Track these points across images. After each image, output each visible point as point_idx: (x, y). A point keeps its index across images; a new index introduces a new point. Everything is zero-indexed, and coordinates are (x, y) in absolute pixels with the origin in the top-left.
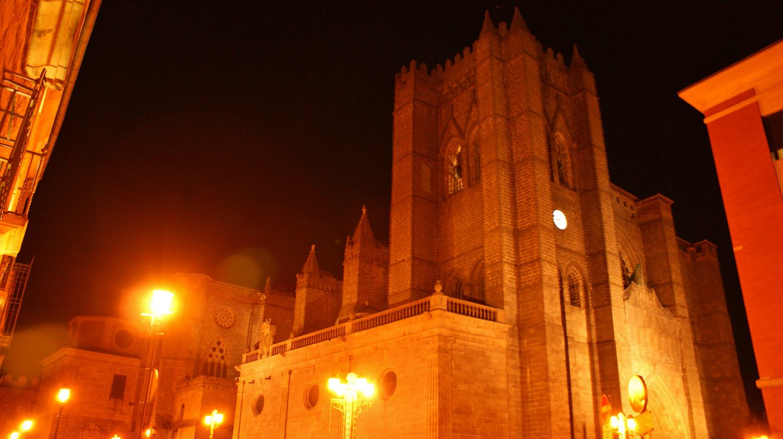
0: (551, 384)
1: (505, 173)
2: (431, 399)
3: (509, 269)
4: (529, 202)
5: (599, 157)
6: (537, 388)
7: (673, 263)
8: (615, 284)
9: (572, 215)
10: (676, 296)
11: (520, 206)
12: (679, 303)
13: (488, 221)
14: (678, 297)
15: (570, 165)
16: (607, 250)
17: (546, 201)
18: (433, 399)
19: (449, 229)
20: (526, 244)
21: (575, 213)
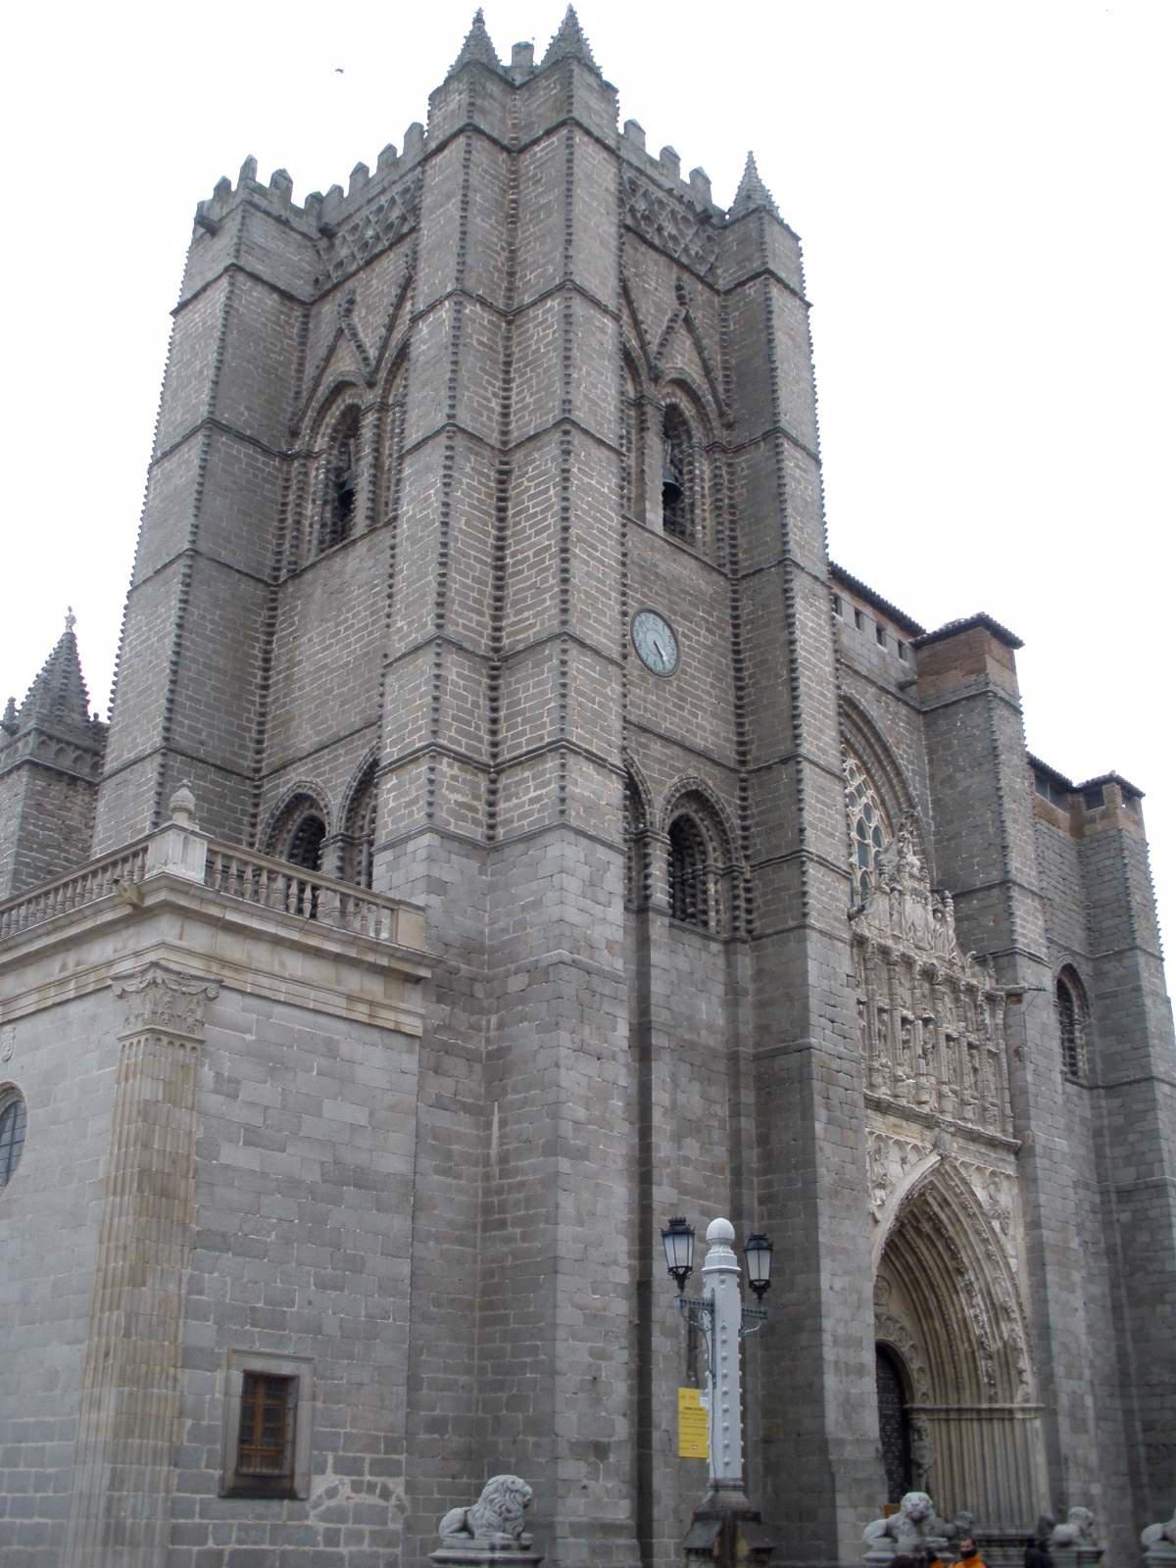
0: (564, 1164)
1: (473, 469)
2: (114, 1194)
3: (456, 771)
4: (543, 561)
5: (797, 466)
6: (519, 1178)
7: (1015, 821)
8: (823, 862)
9: (697, 634)
10: (1018, 921)
12: (1028, 946)
13: (404, 618)
14: (1023, 927)
15: (707, 485)
16: (803, 751)
17: (602, 563)
18: (122, 1195)
19: (300, 662)
20: (522, 695)
21: (708, 630)
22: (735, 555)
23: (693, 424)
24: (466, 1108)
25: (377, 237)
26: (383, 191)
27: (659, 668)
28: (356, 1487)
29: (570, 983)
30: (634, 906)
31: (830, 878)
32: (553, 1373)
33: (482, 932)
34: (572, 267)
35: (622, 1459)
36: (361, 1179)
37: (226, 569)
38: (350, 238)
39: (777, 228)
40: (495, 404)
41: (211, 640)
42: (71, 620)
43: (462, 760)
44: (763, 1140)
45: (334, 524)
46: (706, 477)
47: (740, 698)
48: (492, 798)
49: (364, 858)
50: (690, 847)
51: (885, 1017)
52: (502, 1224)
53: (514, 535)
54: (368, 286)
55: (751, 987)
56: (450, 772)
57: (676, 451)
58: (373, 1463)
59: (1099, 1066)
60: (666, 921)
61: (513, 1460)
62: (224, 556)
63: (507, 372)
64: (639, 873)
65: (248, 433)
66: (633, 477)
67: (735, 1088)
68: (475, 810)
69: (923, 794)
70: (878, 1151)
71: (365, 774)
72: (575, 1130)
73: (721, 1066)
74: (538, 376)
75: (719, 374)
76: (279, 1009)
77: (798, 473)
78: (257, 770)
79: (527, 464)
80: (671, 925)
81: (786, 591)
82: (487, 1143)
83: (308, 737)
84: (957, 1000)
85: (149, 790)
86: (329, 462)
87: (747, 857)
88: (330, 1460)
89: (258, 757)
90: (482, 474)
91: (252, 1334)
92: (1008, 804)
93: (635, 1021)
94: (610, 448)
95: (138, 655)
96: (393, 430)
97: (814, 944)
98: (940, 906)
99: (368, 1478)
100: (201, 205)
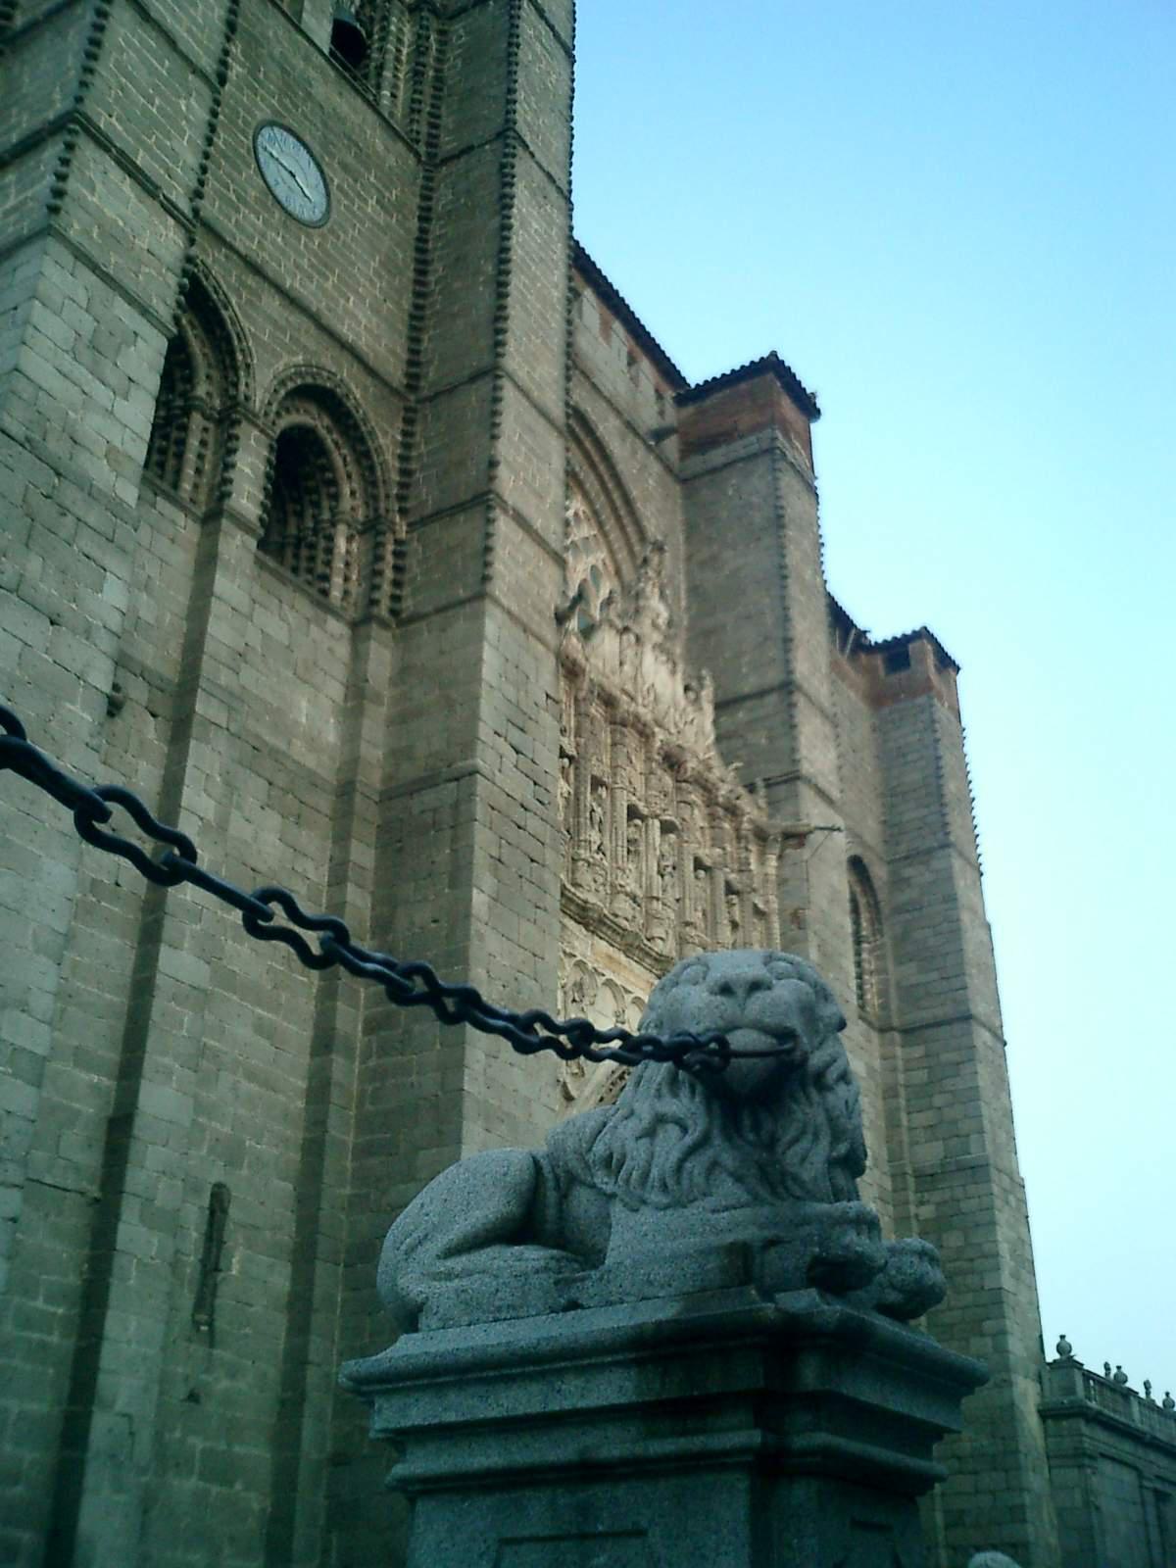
51: (603, 792)
55: (387, 694)
59: (894, 1004)
70: (579, 986)
73: (325, 802)
81: (504, 196)
84: (712, 817)
97: (493, 624)
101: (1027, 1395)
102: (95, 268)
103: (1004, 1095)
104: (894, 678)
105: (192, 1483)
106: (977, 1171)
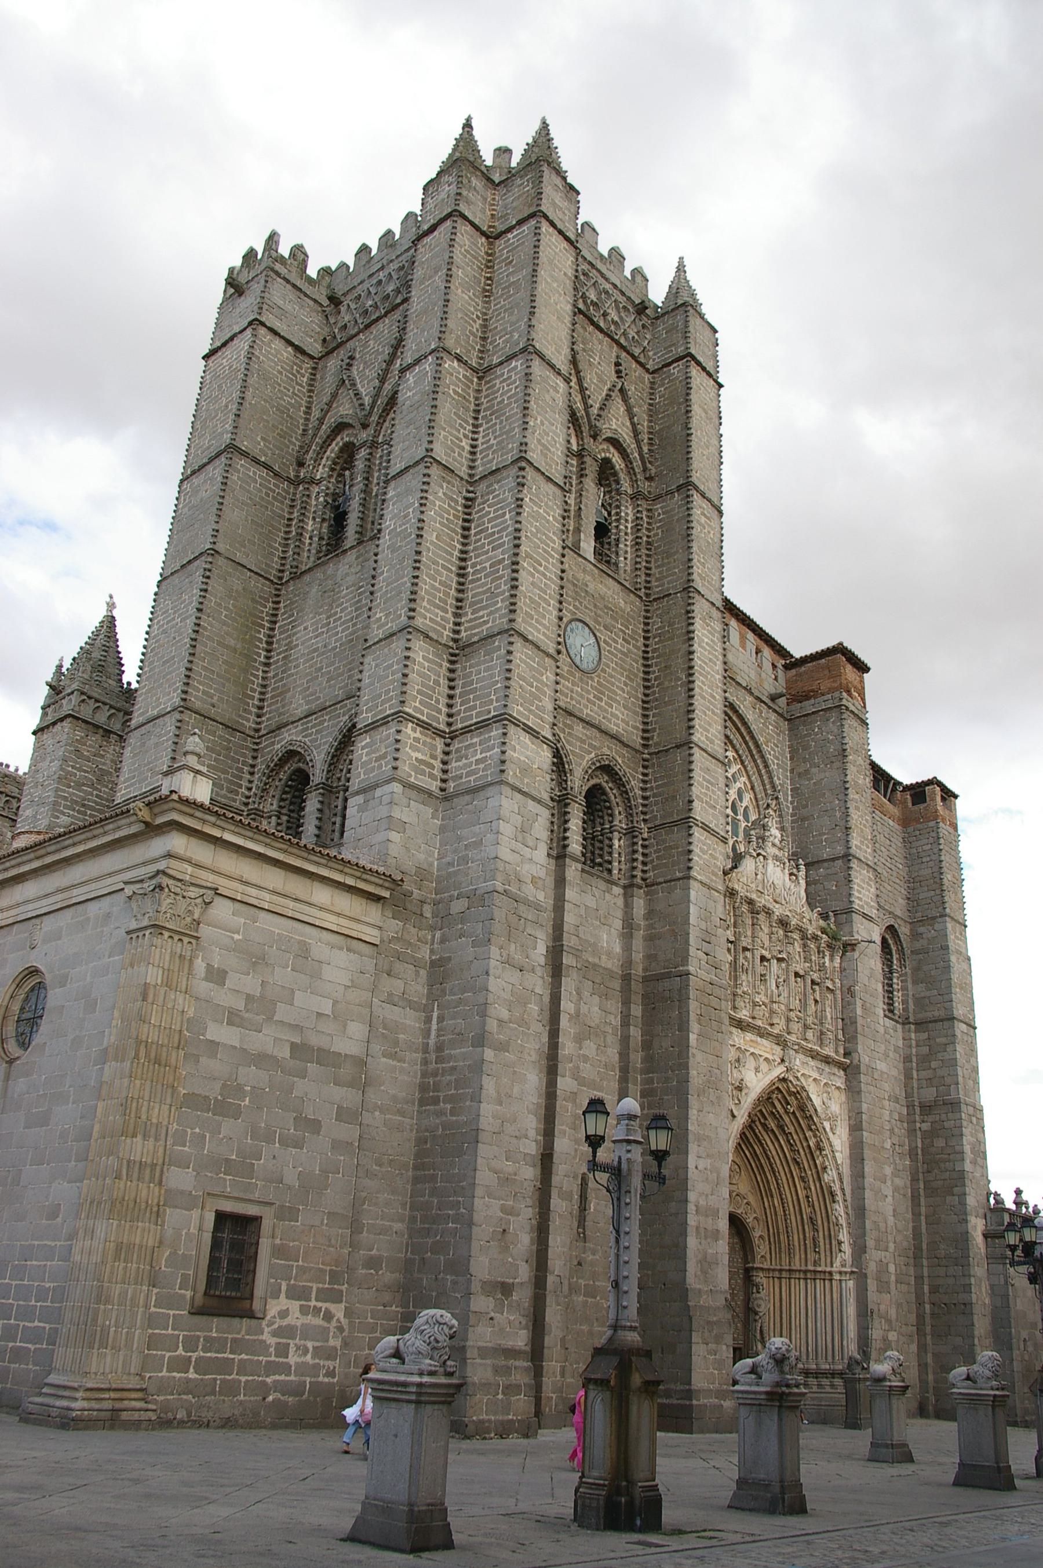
0: (489, 1054)
1: (444, 494)
3: (418, 735)
5: (703, 514)
7: (857, 808)
8: (706, 828)
10: (856, 887)
11: (473, 581)
12: (862, 907)
14: (859, 892)
15: (629, 526)
19: (297, 645)
22: (649, 582)
23: (622, 476)
24: (411, 1004)
25: (376, 306)
26: (382, 268)
27: (584, 666)
28: (304, 1311)
29: (501, 909)
30: (554, 853)
31: (711, 841)
32: (470, 1224)
33: (431, 865)
34: (534, 335)
35: (523, 1296)
36: (324, 1057)
37: (240, 568)
38: (353, 306)
39: (699, 321)
40: (466, 444)
41: (224, 623)
42: (111, 606)
43: (424, 725)
44: (647, 1045)
45: (329, 538)
46: (629, 518)
47: (646, 695)
48: (446, 758)
49: (340, 802)
50: (601, 810)
51: (748, 954)
52: (436, 1101)
53: (475, 549)
54: (365, 345)
56: (413, 735)
57: (607, 497)
58: (318, 1290)
59: (911, 1007)
60: (579, 866)
61: (434, 1294)
62: (239, 557)
63: (476, 419)
64: (559, 827)
65: (263, 459)
66: (572, 513)
67: (626, 1002)
68: (433, 768)
69: (785, 783)
70: (738, 1060)
71: (344, 736)
72: (499, 1026)
73: (617, 984)
74: (501, 422)
75: (645, 437)
76: (263, 915)
77: (703, 520)
78: (257, 730)
79: (488, 494)
80: (583, 870)
82: (427, 1033)
83: (301, 705)
84: (805, 946)
85: (167, 740)
86: (328, 488)
87: (645, 820)
88: (284, 1288)
89: (259, 720)
90: (452, 499)
91: (225, 1180)
92: (852, 794)
93: (550, 944)
94: (556, 484)
95: (165, 632)
96: (381, 464)
97: (695, 892)
98: (795, 871)
99: (313, 1303)
100: (231, 270)
101: (977, 1226)
102: (520, 791)
103: (972, 1060)
104: (916, 807)
105: (581, 1298)
106: (955, 1105)
